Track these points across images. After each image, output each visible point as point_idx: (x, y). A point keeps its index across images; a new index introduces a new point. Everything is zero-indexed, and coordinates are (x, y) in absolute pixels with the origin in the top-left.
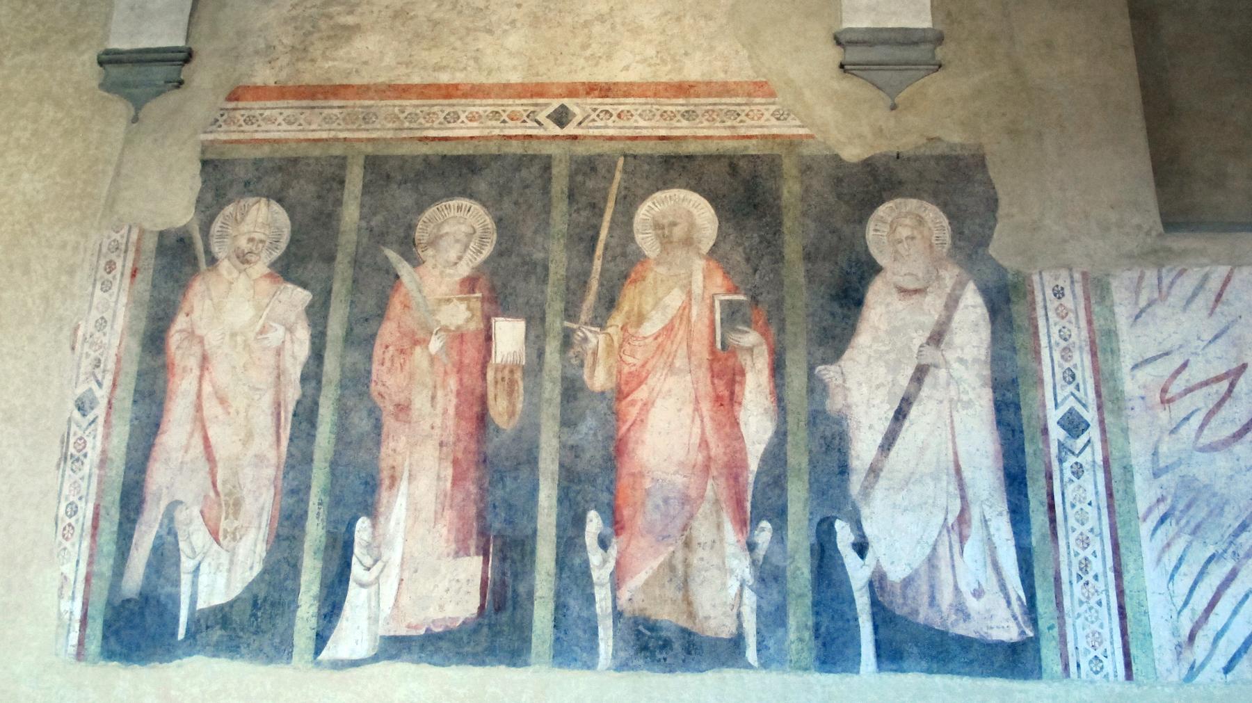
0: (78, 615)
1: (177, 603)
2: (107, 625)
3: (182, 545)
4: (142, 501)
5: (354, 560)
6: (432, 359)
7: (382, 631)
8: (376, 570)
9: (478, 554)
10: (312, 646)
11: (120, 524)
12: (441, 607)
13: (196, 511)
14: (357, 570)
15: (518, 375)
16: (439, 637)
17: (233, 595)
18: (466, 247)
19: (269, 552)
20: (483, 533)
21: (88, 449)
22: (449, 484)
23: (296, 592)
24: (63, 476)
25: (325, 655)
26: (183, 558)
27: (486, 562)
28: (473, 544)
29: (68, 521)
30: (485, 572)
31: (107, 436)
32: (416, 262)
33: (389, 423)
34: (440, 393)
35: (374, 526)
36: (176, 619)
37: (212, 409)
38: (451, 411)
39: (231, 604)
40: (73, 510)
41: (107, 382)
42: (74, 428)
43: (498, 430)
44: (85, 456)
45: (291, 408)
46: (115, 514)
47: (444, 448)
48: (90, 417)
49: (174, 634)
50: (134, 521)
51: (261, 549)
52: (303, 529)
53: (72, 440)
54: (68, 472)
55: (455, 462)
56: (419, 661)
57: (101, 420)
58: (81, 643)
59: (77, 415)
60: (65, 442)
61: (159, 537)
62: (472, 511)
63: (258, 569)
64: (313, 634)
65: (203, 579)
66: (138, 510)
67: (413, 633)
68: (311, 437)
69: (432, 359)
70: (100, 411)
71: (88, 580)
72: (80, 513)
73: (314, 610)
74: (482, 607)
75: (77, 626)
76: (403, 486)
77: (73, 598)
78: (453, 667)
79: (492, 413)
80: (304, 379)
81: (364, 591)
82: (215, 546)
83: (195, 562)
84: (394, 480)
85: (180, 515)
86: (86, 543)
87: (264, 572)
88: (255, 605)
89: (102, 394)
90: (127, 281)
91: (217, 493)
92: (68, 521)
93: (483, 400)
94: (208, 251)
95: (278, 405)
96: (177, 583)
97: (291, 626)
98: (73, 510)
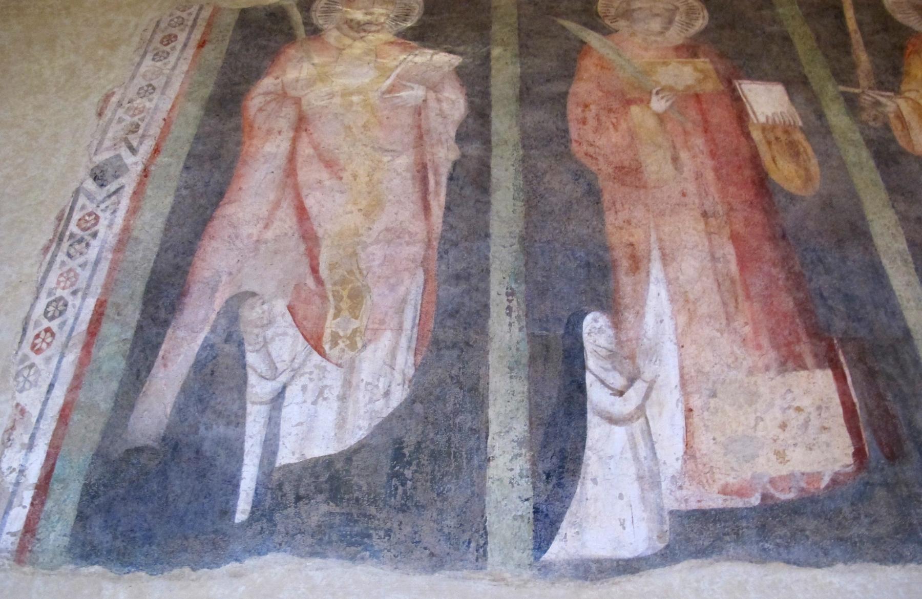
0: (34, 474)
1: (236, 454)
2: (89, 494)
3: (252, 358)
4: (183, 293)
5: (589, 378)
6: (661, 118)
7: (670, 504)
8: (634, 396)
9: (820, 366)
10: (526, 532)
11: (140, 328)
12: (781, 456)
13: (280, 306)
14: (596, 394)
15: (799, 136)
16: (794, 509)
17: (351, 441)
18: (670, 22)
19: (421, 369)
20: (817, 333)
21: (101, 228)
22: (734, 268)
23: (481, 432)
24: (51, 264)
25: (556, 551)
26: (252, 379)
27: (840, 378)
28: (805, 348)
29: (46, 324)
30: (844, 394)
31: (133, 211)
32: (606, 32)
33: (610, 190)
34: (684, 155)
35: (617, 325)
36: (232, 483)
37: (309, 173)
38: (710, 176)
39: (349, 456)
40: (58, 308)
41: (146, 148)
42: (82, 200)
43: (792, 198)
44: (94, 235)
45: (445, 171)
46: (133, 314)
47: (712, 221)
48: (112, 187)
49: (227, 512)
50: (166, 324)
51: (405, 362)
52: (483, 331)
53: (76, 216)
54: (61, 257)
55: (735, 238)
56: (763, 558)
57: (128, 191)
58: (30, 528)
59: (90, 185)
60: (63, 219)
61: (207, 346)
62: (787, 303)
63: (399, 395)
64: (526, 509)
65: (292, 412)
66: (175, 308)
67: (737, 503)
68: (483, 205)
69: (661, 118)
70: (129, 182)
71: (64, 416)
72: (70, 314)
73: (522, 464)
74: (859, 453)
75: (27, 496)
76: (656, 269)
77: (30, 447)
78: (840, 566)
79: (775, 176)
80: (462, 137)
81: (619, 432)
82: (316, 358)
83: (277, 384)
84: (637, 263)
85: (251, 313)
86: (72, 357)
87: (412, 401)
88: (398, 455)
89: (134, 163)
90: (190, 52)
91: (319, 281)
92: (46, 324)
93: (755, 160)
94: (308, 23)
95: (422, 173)
96: (238, 420)
97: (480, 495)
98: (58, 308)
